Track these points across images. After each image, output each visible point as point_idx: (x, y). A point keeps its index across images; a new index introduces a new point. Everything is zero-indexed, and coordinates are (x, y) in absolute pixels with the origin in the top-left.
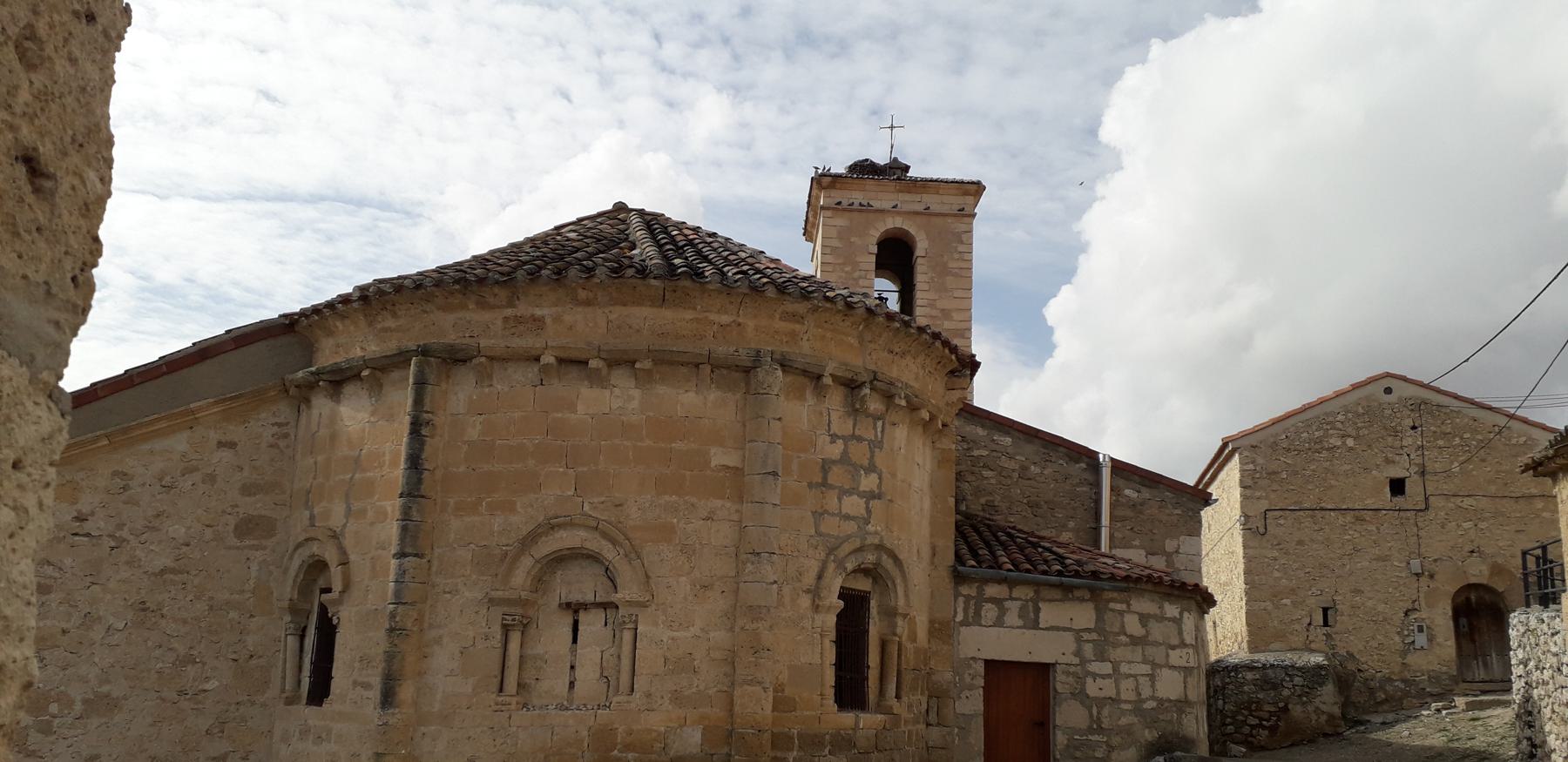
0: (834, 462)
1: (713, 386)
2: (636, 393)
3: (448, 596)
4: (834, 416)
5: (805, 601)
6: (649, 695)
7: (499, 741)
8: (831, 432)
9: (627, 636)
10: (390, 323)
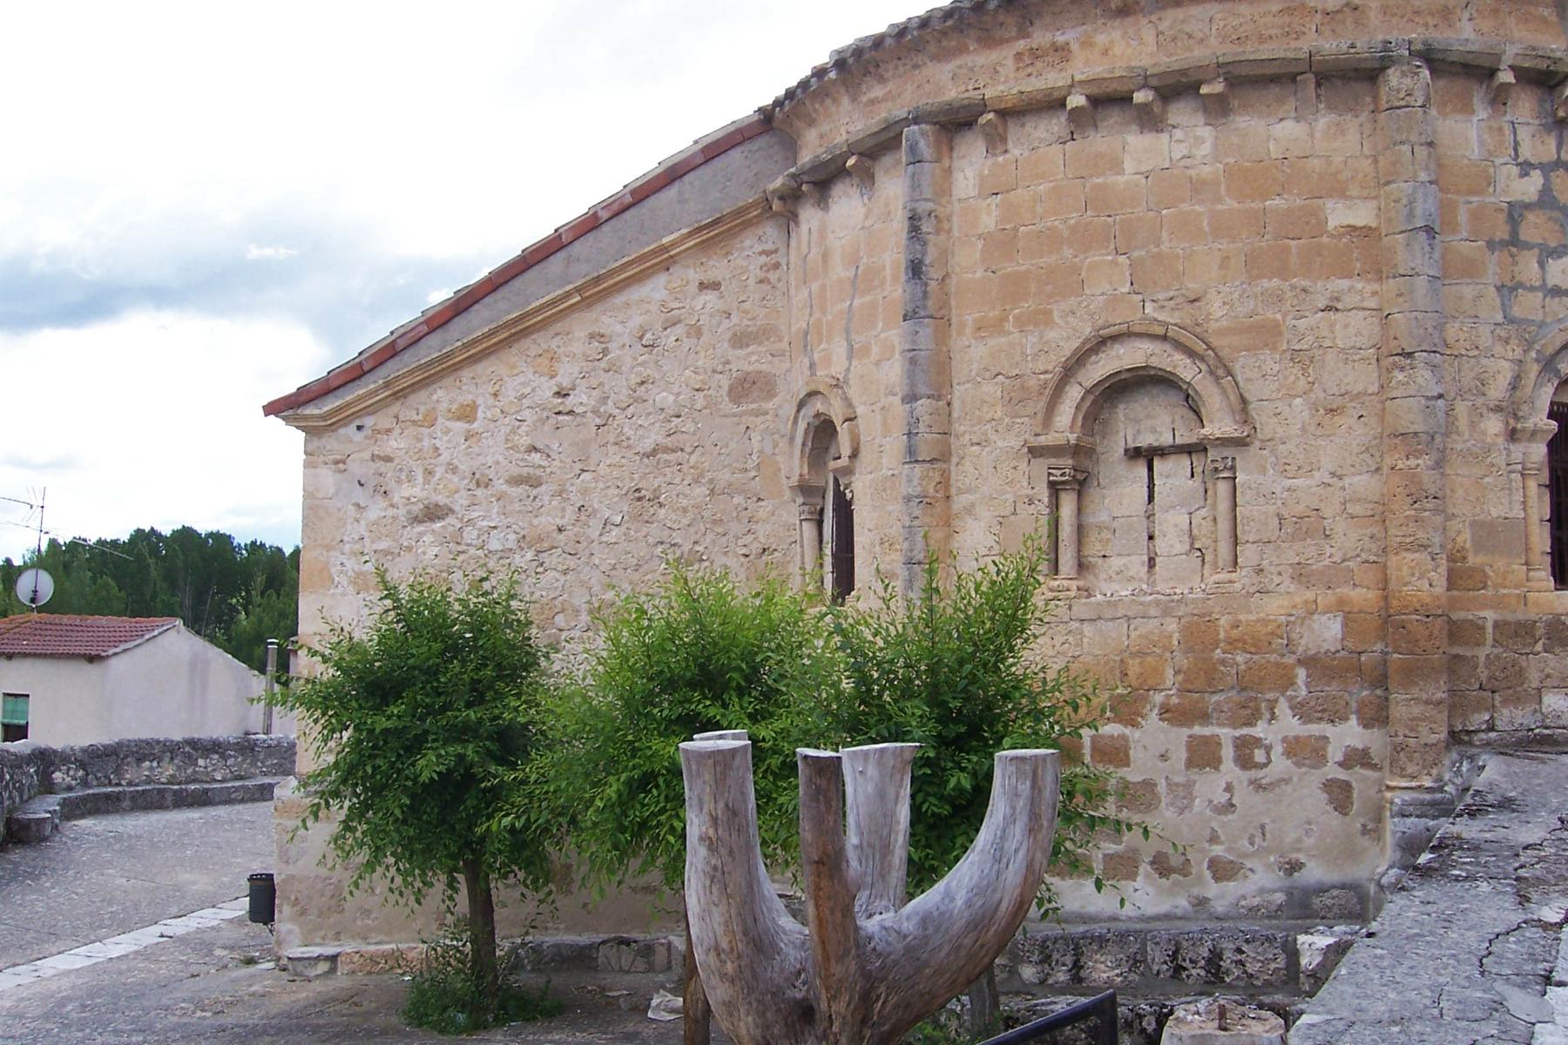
0: (1528, 206)
1: (1322, 106)
2: (1206, 132)
3: (975, 448)
4: (1524, 134)
5: (1494, 426)
6: (1260, 571)
7: (1059, 640)
8: (1520, 160)
9: (1223, 488)
10: (878, 91)
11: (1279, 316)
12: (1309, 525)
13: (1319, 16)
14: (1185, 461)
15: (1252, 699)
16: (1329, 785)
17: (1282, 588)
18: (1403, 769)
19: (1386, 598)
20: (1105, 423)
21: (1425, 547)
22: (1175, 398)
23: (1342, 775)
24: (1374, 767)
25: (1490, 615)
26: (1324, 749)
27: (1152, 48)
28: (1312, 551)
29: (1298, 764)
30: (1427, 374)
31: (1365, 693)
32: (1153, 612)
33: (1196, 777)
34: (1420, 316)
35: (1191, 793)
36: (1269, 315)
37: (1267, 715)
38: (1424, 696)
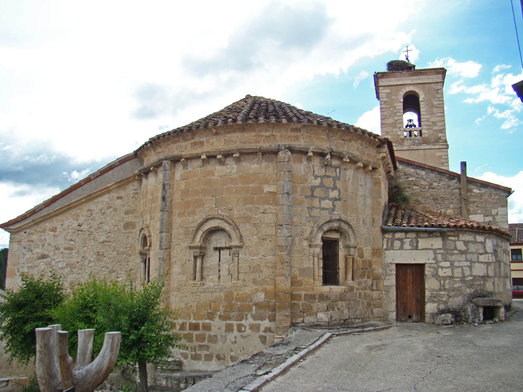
0: (316, 187)
1: (264, 160)
2: (235, 166)
3: (177, 246)
4: (316, 168)
5: (306, 243)
6: (244, 280)
7: (195, 297)
8: (315, 175)
9: (236, 259)
11: (251, 214)
12: (257, 269)
13: (264, 137)
14: (228, 251)
15: (242, 314)
16: (261, 337)
17: (250, 285)
18: (278, 333)
19: (275, 288)
20: (209, 240)
21: (284, 275)
22: (226, 235)
23: (264, 334)
24: (272, 332)
25: (303, 293)
26: (259, 327)
27: (223, 144)
28: (257, 276)
29: (253, 331)
30: (286, 231)
31: (270, 313)
32: (218, 290)
33: (227, 334)
34: (285, 216)
35: (226, 338)
36: (248, 214)
37: (245, 318)
38: (283, 314)
